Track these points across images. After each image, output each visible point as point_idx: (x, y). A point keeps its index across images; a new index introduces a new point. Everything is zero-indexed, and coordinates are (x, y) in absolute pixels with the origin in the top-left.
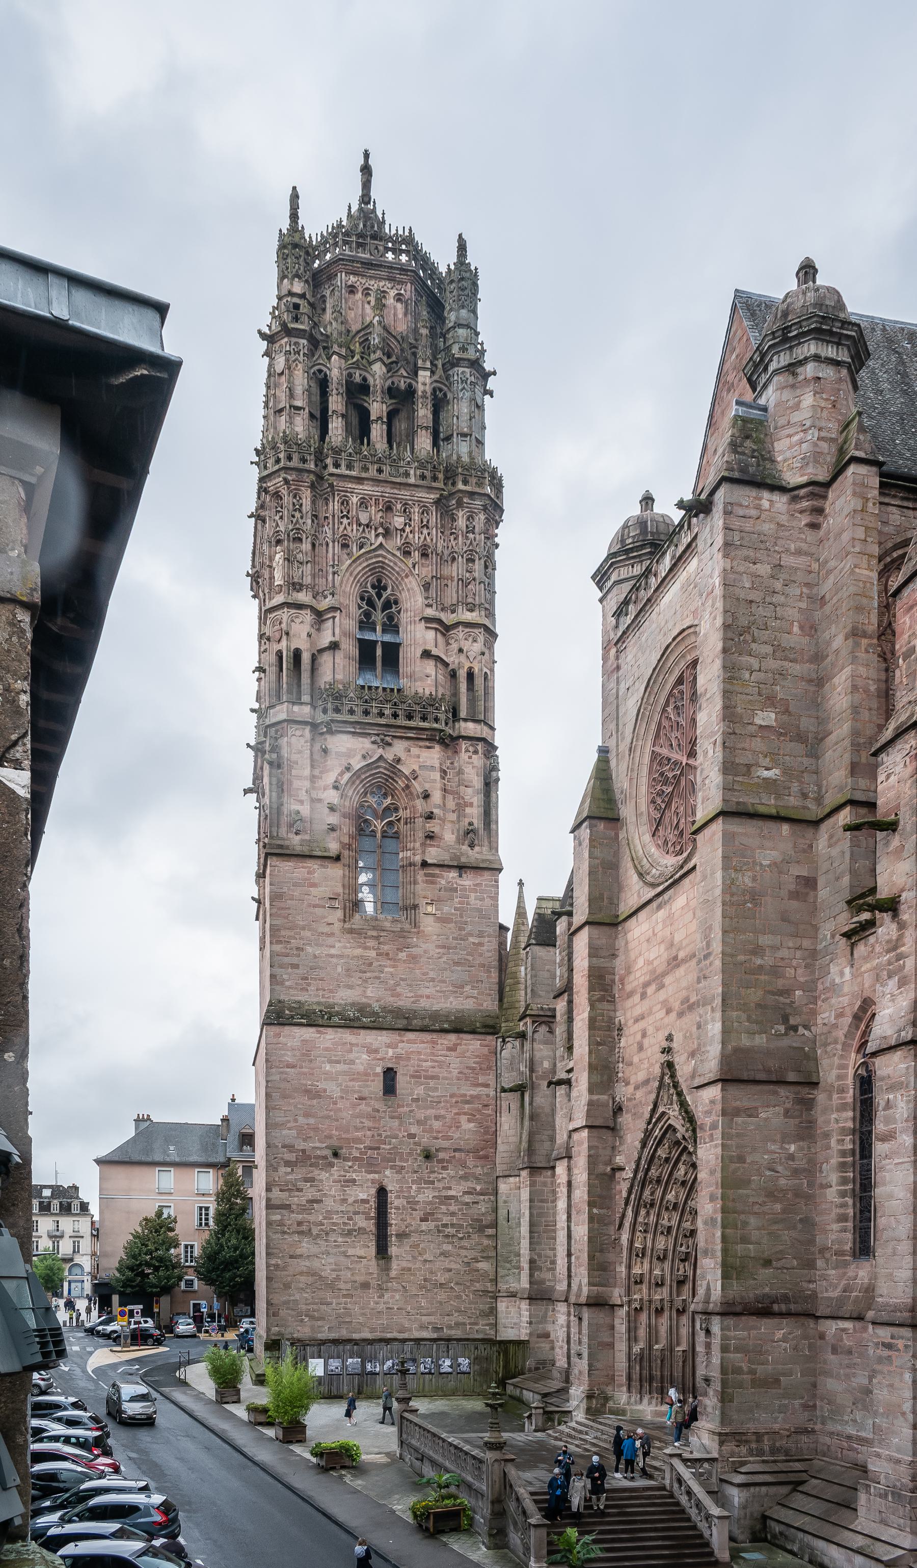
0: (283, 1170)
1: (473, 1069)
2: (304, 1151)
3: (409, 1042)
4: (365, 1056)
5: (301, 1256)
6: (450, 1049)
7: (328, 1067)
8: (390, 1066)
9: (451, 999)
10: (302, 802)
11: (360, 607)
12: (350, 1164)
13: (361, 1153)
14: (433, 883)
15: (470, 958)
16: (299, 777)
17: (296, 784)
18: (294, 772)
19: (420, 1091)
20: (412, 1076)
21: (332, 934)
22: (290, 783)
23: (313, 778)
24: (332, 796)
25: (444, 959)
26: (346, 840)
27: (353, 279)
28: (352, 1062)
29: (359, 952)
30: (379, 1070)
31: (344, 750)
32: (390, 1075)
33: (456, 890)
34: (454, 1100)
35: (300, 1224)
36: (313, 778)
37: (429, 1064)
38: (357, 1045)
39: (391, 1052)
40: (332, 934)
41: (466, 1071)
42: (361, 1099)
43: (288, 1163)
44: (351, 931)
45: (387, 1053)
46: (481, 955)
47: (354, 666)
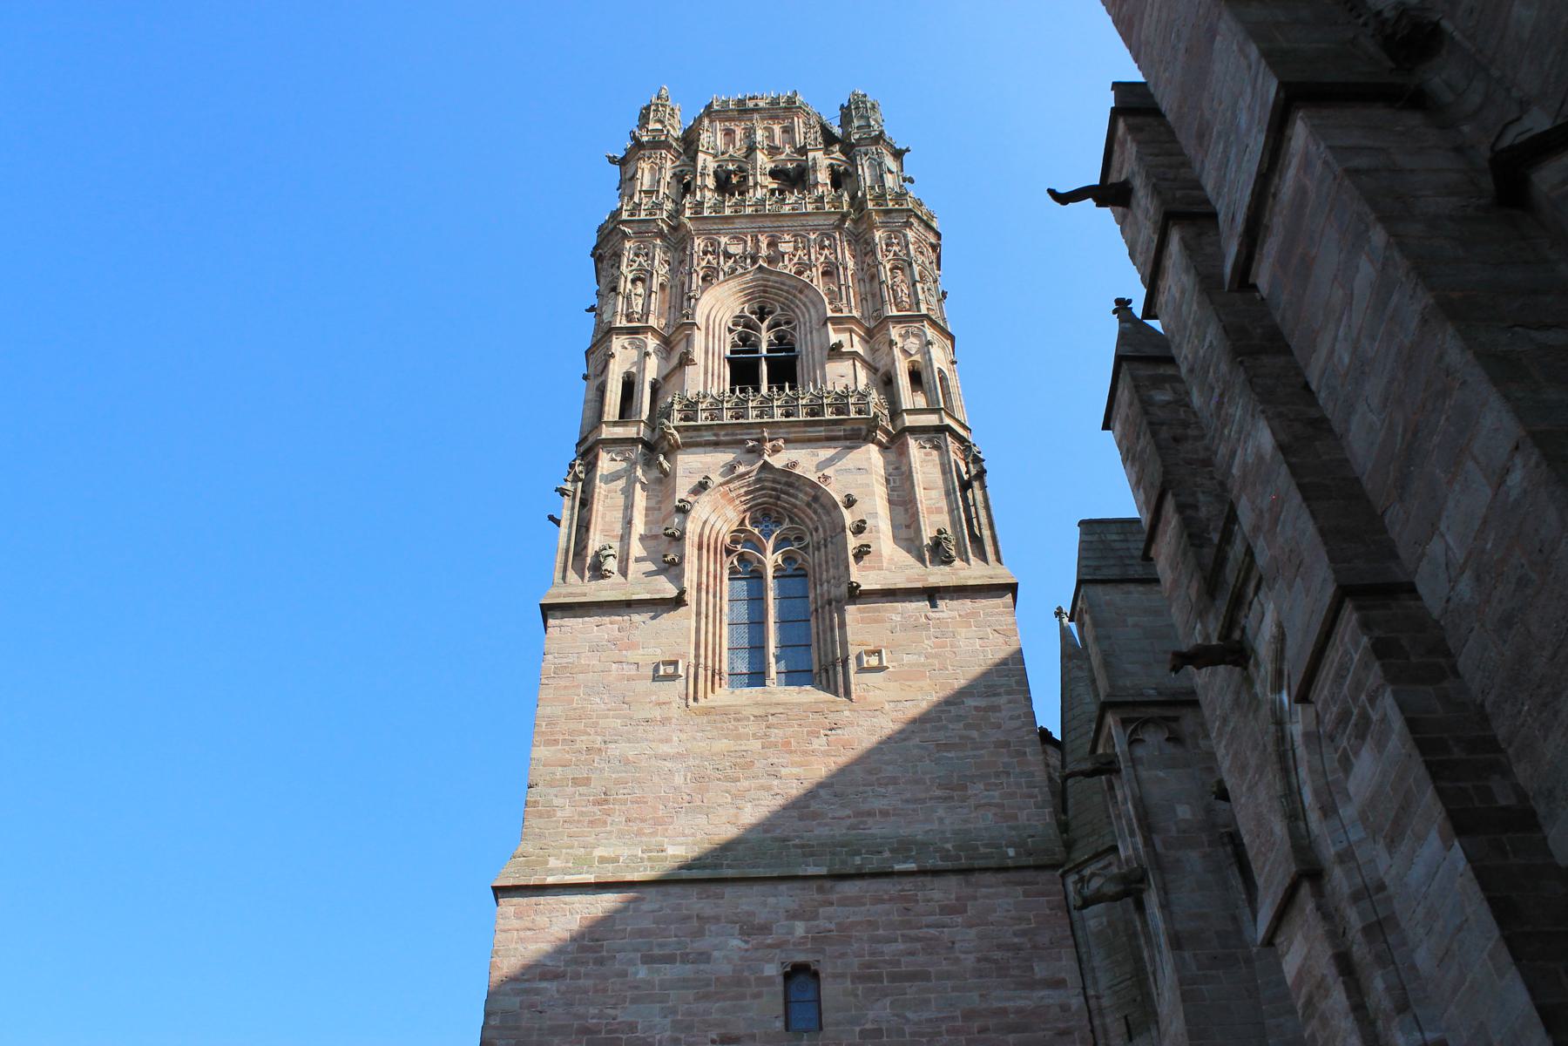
1: (1017, 948)
3: (844, 902)
4: (736, 943)
6: (946, 910)
7: (642, 972)
8: (800, 958)
9: (941, 812)
11: (731, 331)
14: (876, 621)
15: (975, 734)
19: (880, 1012)
20: (857, 978)
21: (665, 721)
28: (704, 957)
29: (723, 745)
30: (772, 970)
31: (700, 465)
32: (799, 974)
33: (926, 627)
34: (976, 1025)
37: (901, 946)
38: (717, 919)
39: (800, 928)
40: (665, 721)
41: (997, 955)
45: (791, 932)
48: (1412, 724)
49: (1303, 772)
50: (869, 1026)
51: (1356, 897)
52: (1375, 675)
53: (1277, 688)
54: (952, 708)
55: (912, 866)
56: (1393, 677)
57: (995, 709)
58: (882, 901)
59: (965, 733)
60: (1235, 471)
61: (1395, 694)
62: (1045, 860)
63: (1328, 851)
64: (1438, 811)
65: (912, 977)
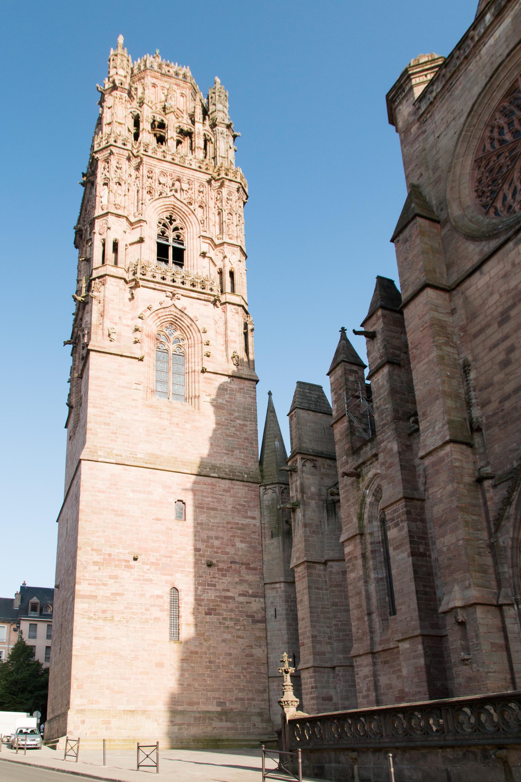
1: (244, 506)
2: (110, 555)
6: (224, 491)
9: (225, 458)
12: (148, 567)
13: (157, 559)
15: (238, 433)
25: (220, 432)
41: (238, 507)
42: (158, 519)
43: (95, 563)
46: (246, 432)
48: (409, 531)
49: (366, 510)
50: (199, 522)
51: (371, 543)
52: (404, 517)
53: (366, 489)
54: (232, 422)
55: (216, 475)
56: (408, 519)
57: (246, 425)
58: (206, 484)
59: (235, 432)
60: (382, 445)
61: (408, 524)
62: (256, 481)
63: (367, 531)
64: (409, 550)
65: (213, 509)
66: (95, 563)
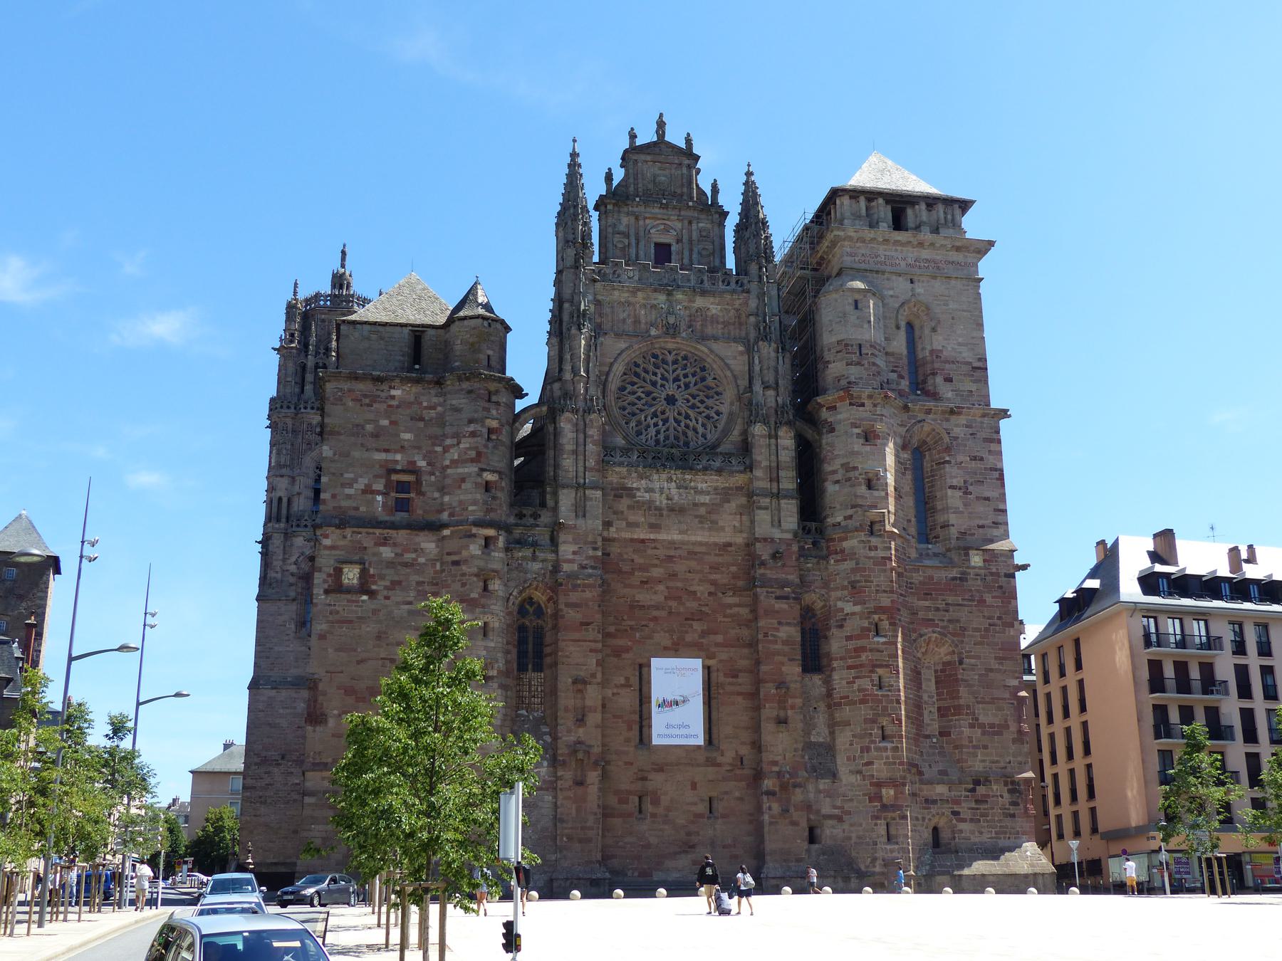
0: (253, 767)
2: (265, 757)
4: (302, 705)
5: (260, 816)
10: (277, 572)
16: (276, 560)
17: (275, 563)
18: (274, 557)
22: (272, 563)
23: (284, 560)
24: (293, 568)
26: (300, 590)
27: (323, 316)
28: (295, 708)
35: (260, 797)
36: (284, 560)
42: (299, 727)
43: (256, 764)
44: (299, 638)
47: (310, 503)
66: (256, 764)
